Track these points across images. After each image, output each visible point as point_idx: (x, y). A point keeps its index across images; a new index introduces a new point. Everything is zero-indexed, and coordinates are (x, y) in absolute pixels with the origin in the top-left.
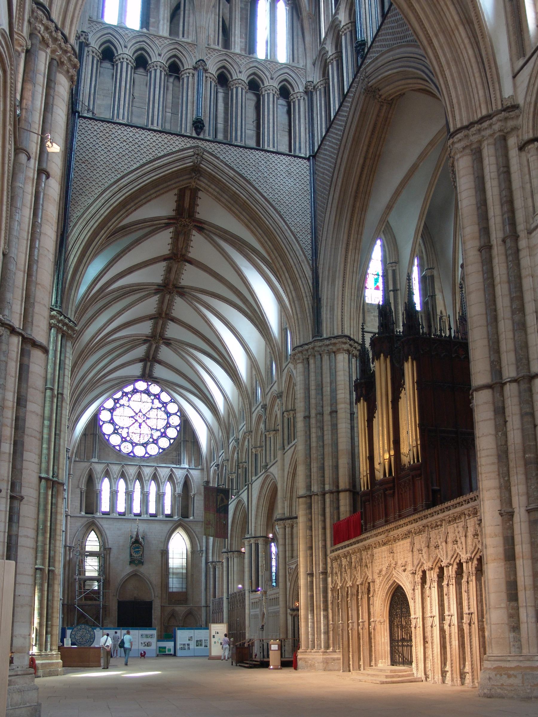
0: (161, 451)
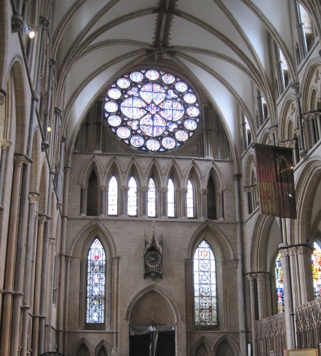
0: (178, 145)
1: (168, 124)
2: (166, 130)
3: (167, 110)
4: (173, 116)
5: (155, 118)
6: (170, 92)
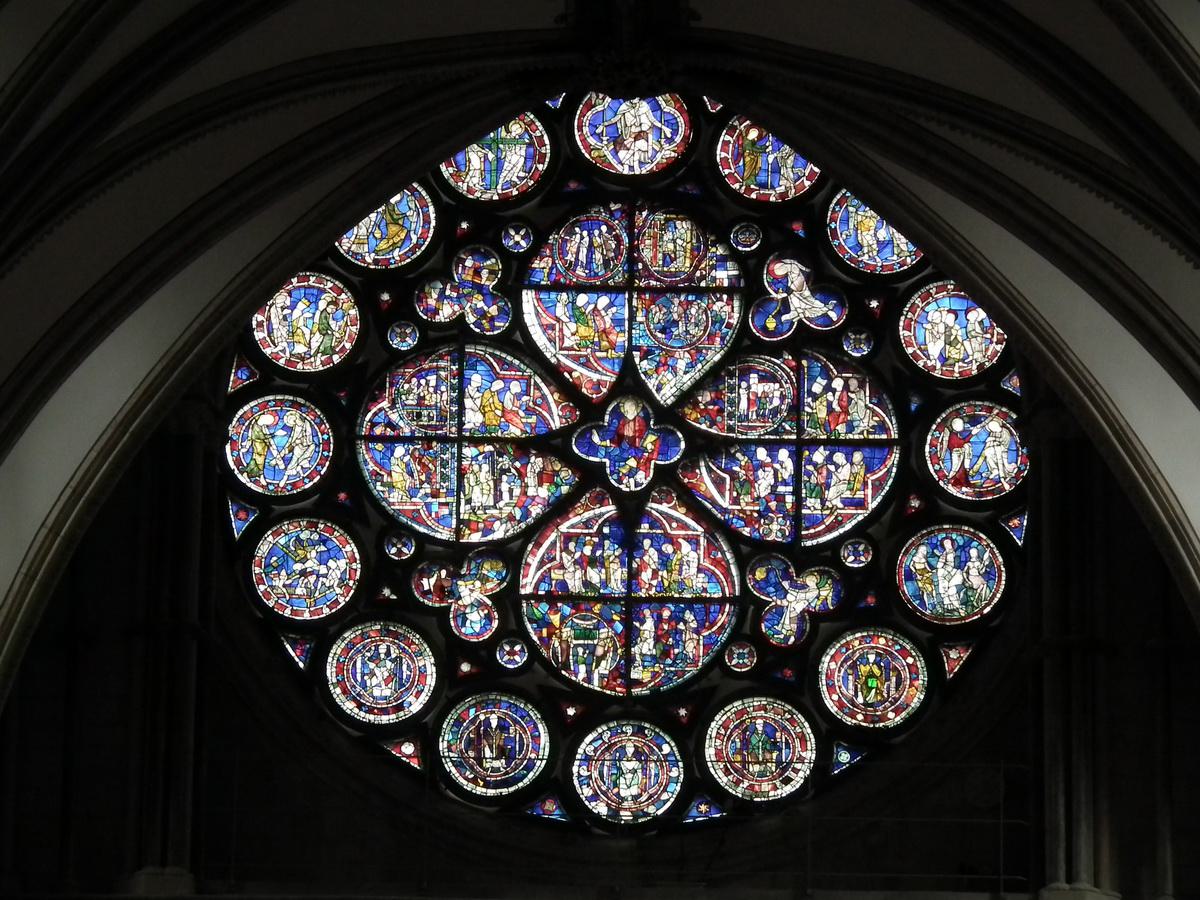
1: (760, 574)
2: (736, 638)
3: (747, 446)
4: (799, 503)
5: (645, 528)
6: (782, 282)
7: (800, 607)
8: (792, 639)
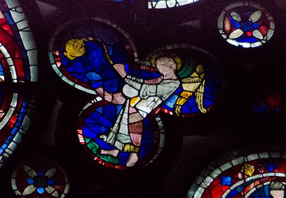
1: (73, 50)
7: (146, 108)
8: (134, 158)
